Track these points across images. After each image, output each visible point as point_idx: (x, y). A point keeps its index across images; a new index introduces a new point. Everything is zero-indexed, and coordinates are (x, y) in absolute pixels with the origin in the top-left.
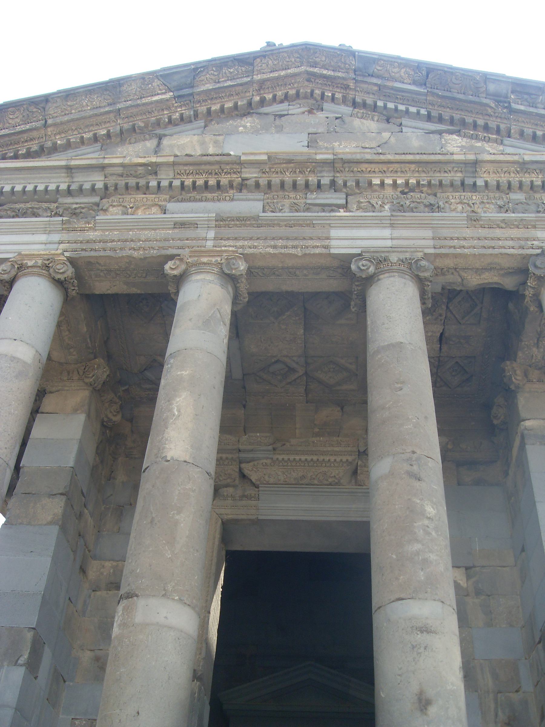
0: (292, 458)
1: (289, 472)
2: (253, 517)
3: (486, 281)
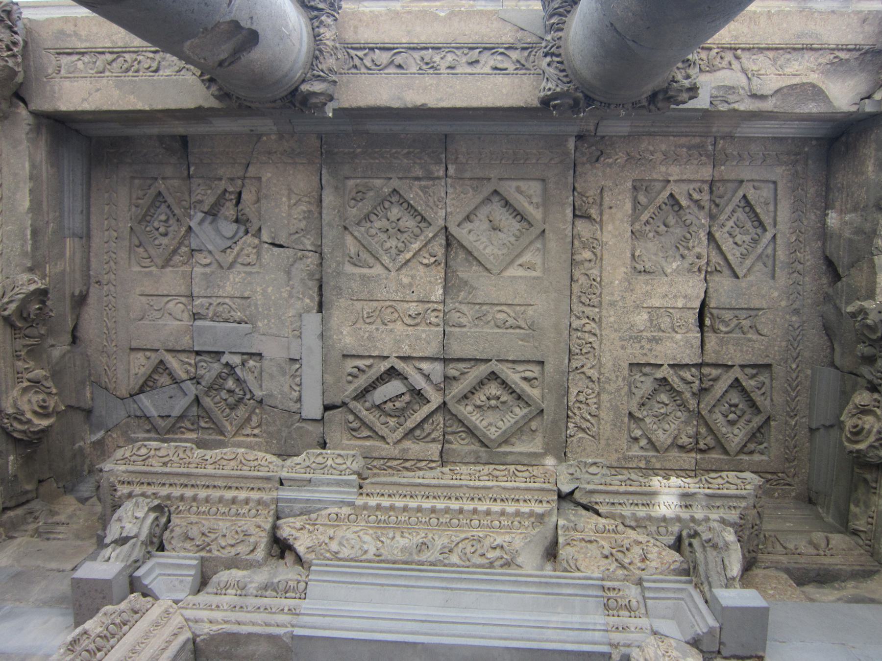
0: (399, 503)
1: (391, 535)
2: (280, 631)
3: (796, 80)
